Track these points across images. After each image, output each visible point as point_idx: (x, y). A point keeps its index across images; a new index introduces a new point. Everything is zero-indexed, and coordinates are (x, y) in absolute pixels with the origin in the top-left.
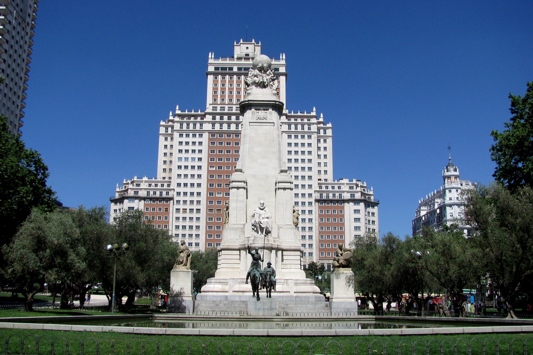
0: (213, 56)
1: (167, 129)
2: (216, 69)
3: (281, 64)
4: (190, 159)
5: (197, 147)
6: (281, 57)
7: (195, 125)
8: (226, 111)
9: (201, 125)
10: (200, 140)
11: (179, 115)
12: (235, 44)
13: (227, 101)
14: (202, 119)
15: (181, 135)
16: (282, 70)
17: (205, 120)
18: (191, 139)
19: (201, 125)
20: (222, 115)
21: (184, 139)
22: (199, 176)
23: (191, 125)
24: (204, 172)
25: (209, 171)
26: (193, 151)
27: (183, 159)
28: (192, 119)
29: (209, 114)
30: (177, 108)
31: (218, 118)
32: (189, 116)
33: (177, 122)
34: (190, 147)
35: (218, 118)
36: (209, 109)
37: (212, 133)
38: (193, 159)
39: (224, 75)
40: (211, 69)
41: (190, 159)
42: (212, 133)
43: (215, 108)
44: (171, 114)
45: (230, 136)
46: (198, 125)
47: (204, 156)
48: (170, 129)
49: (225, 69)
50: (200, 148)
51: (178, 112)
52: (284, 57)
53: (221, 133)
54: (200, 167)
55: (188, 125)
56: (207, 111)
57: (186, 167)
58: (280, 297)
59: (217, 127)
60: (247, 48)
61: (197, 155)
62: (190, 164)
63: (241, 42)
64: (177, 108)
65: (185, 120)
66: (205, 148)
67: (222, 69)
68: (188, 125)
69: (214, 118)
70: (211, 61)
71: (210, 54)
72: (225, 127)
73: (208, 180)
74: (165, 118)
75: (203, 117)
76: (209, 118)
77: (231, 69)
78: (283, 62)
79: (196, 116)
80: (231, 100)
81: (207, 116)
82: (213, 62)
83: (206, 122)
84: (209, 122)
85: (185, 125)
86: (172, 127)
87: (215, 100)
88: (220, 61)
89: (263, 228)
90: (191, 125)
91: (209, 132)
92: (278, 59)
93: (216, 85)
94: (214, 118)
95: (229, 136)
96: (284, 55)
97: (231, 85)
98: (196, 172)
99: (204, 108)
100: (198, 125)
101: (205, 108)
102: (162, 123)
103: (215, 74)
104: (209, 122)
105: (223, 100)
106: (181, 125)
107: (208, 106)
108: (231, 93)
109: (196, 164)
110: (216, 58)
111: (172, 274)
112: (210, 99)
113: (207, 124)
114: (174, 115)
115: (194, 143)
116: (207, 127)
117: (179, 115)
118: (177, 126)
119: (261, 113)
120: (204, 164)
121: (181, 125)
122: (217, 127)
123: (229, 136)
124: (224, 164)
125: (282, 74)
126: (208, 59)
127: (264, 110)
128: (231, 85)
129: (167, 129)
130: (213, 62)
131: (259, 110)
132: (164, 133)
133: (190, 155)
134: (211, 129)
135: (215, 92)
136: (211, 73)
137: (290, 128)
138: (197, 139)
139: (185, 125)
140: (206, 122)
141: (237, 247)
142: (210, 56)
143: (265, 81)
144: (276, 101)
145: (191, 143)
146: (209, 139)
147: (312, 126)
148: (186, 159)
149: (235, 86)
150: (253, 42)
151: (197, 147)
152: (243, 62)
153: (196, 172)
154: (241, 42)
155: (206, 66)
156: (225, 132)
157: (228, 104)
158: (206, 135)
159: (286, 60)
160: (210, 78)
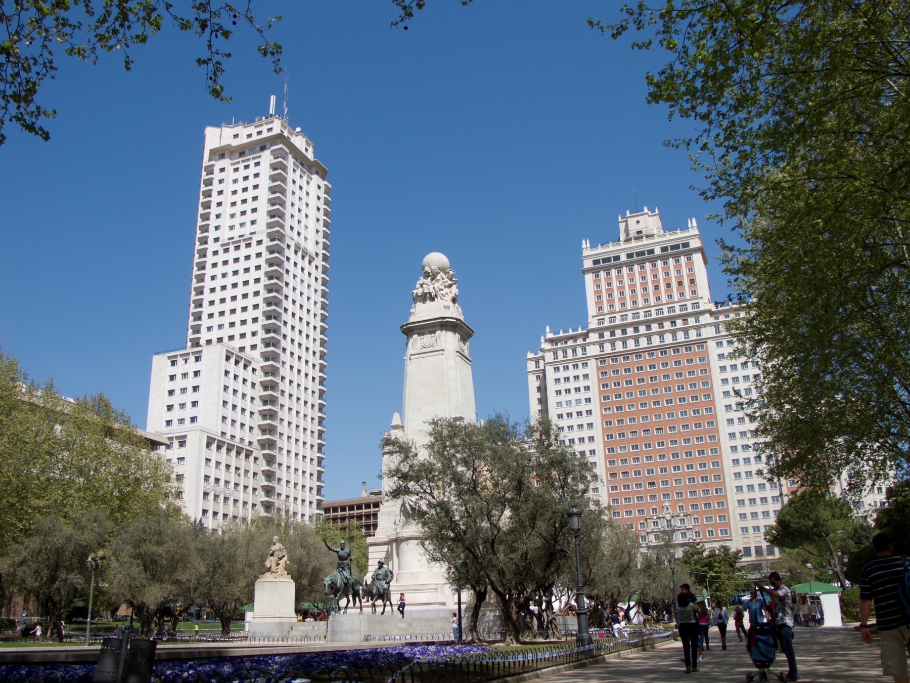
0: (588, 245)
1: (537, 362)
2: (596, 262)
3: (691, 235)
4: (574, 403)
5: (582, 383)
6: (690, 225)
7: (574, 351)
8: (642, 318)
9: (584, 349)
10: (585, 371)
11: (551, 341)
12: (620, 220)
13: (629, 305)
14: (584, 340)
15: (557, 369)
16: (695, 243)
17: (588, 340)
18: (571, 373)
19: (584, 349)
20: (600, 331)
21: (562, 374)
22: (590, 425)
23: (570, 352)
24: (596, 419)
25: (602, 416)
26: (578, 390)
27: (564, 404)
28: (580, 341)
29: (593, 330)
30: (548, 329)
31: (607, 335)
32: (566, 339)
33: (549, 350)
34: (572, 385)
35: (607, 335)
36: (593, 324)
37: (601, 359)
38: (578, 401)
39: (607, 270)
40: (588, 264)
41: (574, 403)
42: (601, 359)
43: (601, 321)
44: (542, 340)
45: (628, 358)
46: (579, 351)
47: (594, 394)
48: (541, 362)
49: (608, 260)
50: (586, 383)
51: (550, 336)
52: (695, 224)
53: (614, 357)
54: (589, 412)
55: (565, 352)
56: (591, 326)
57: (570, 415)
58: (422, 611)
59: (608, 348)
60: (638, 222)
61: (583, 395)
62: (574, 409)
63: (628, 215)
64: (548, 329)
65: (559, 345)
66: (593, 382)
67: (605, 260)
68: (565, 352)
69: (601, 336)
70: (585, 253)
71: (584, 242)
72: (656, 341)
73: (603, 429)
74: (537, 348)
75: (585, 336)
76: (594, 337)
77: (617, 258)
78: (696, 232)
79: (574, 338)
80: (623, 304)
81: (591, 335)
82: (589, 252)
83: (589, 344)
84: (594, 343)
85: (560, 353)
86: (543, 358)
87: (600, 308)
88: (600, 250)
90: (570, 352)
91: (597, 358)
92: (685, 228)
93: (598, 286)
94: (601, 336)
95: (615, 360)
96: (694, 220)
97: (632, 280)
98: (584, 420)
99: (585, 324)
100: (579, 351)
101: (587, 324)
102: (530, 355)
103: (595, 272)
104: (594, 343)
105: (612, 306)
106: (555, 354)
107: (590, 319)
108: (633, 291)
109: (584, 407)
110: (593, 246)
111: (257, 586)
112: (592, 309)
113: (592, 346)
114: (546, 341)
115: (576, 378)
116: (593, 350)
117: (551, 341)
118: (549, 357)
119: (428, 339)
120: (595, 406)
121: (555, 354)
122: (608, 348)
123: (615, 360)
124: (624, 402)
125: (696, 250)
126: (581, 250)
127: (431, 333)
128: (632, 280)
129: (537, 362)
130: (589, 252)
131: (423, 334)
132: (534, 369)
133: (573, 396)
134: (599, 353)
135: (599, 297)
136: (588, 271)
137: (718, 331)
138: (581, 371)
139: (560, 353)
140: (589, 344)
141: (385, 540)
142: (584, 246)
143: (431, 290)
144: (443, 318)
145: (572, 379)
146: (598, 368)
147: (703, 330)
148: (569, 403)
149: (626, 282)
150: (646, 210)
151: (582, 383)
152: (633, 244)
153: (584, 420)
154: (628, 215)
155: (580, 259)
156: (620, 354)
157: (188, 354)
158: (592, 363)
159: (699, 227)
160: (589, 278)
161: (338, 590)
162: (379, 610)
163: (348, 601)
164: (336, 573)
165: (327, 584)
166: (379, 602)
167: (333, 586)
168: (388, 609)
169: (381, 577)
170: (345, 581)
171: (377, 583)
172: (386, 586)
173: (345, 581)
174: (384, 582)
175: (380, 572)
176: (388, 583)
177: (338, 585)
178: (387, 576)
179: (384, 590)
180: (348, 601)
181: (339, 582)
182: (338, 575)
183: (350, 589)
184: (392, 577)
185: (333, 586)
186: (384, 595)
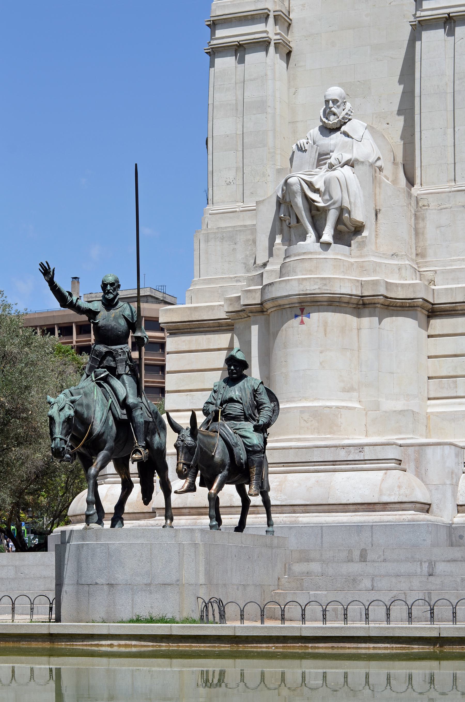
89: (324, 211)
161: (95, 444)
162: (230, 520)
163: (127, 487)
164: (87, 383)
165: (59, 419)
166: (229, 494)
167: (78, 424)
168: (256, 520)
169: (235, 409)
170: (122, 414)
171: (227, 427)
172: (256, 439)
173: (122, 414)
174: (248, 427)
175: (234, 392)
176: (262, 429)
177: (98, 427)
178: (258, 406)
179: (251, 451)
180: (127, 487)
181: (100, 418)
182: (97, 393)
183: (132, 444)
184: (276, 411)
185: (78, 424)
186: (246, 470)
